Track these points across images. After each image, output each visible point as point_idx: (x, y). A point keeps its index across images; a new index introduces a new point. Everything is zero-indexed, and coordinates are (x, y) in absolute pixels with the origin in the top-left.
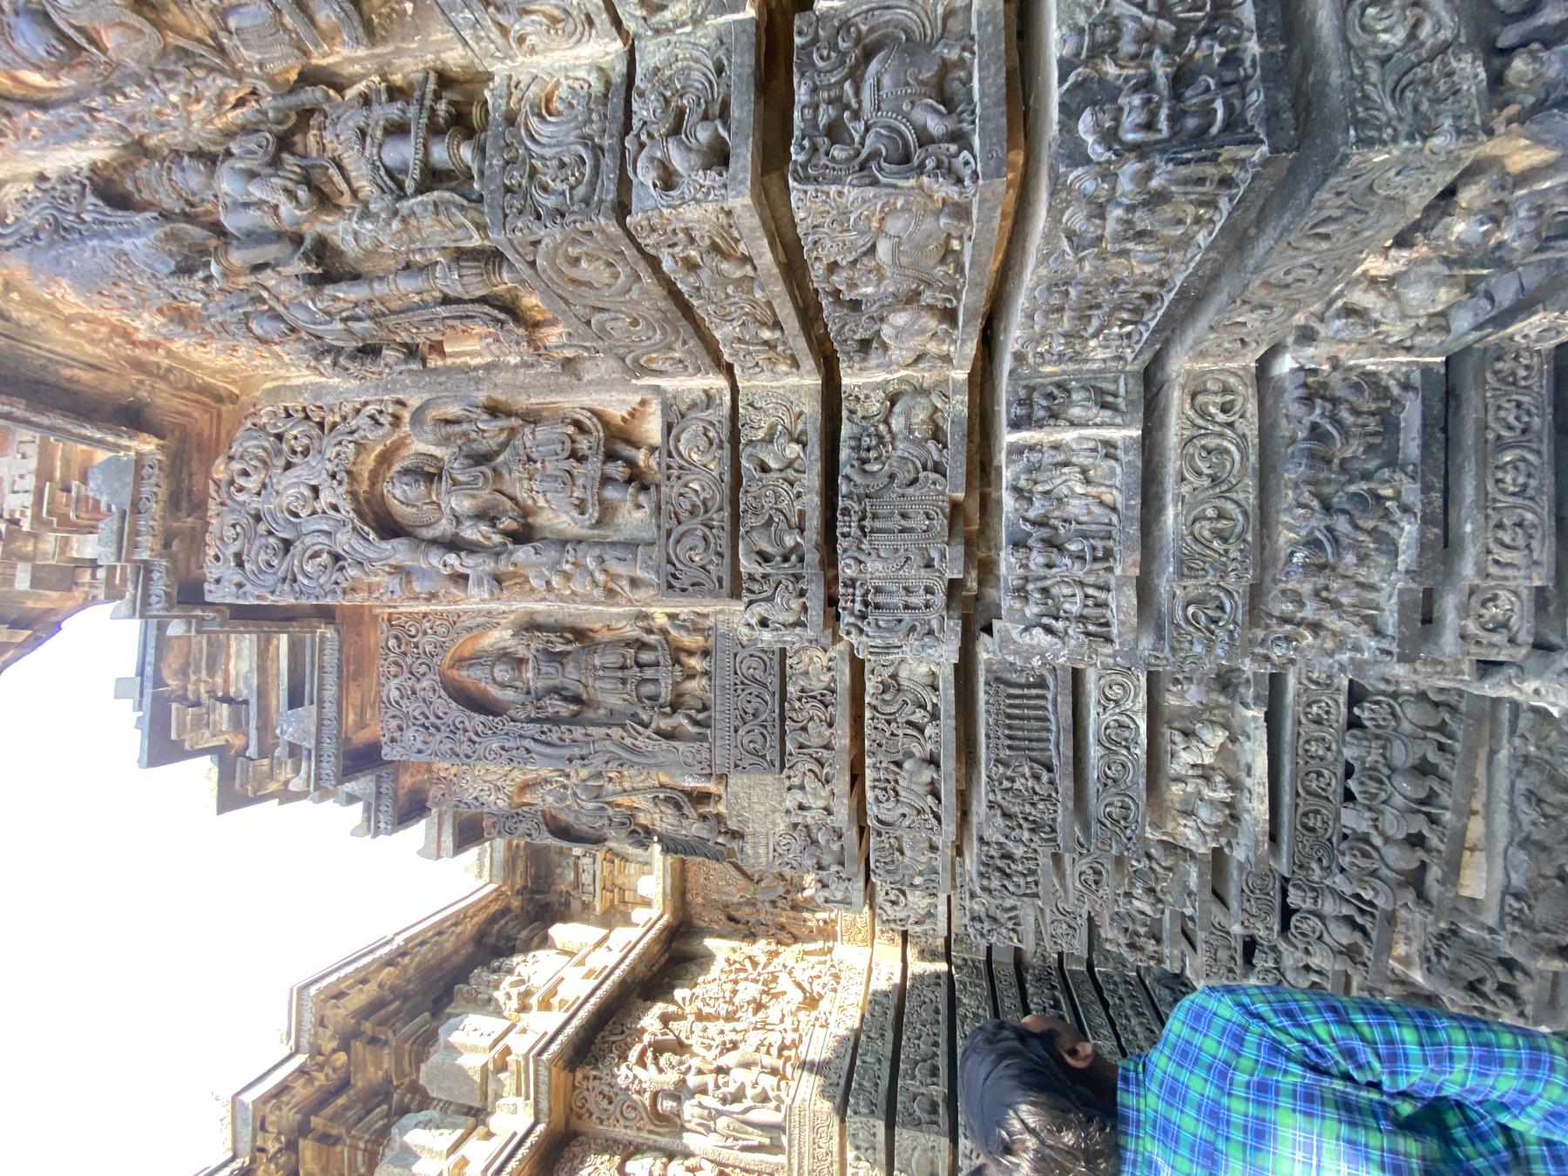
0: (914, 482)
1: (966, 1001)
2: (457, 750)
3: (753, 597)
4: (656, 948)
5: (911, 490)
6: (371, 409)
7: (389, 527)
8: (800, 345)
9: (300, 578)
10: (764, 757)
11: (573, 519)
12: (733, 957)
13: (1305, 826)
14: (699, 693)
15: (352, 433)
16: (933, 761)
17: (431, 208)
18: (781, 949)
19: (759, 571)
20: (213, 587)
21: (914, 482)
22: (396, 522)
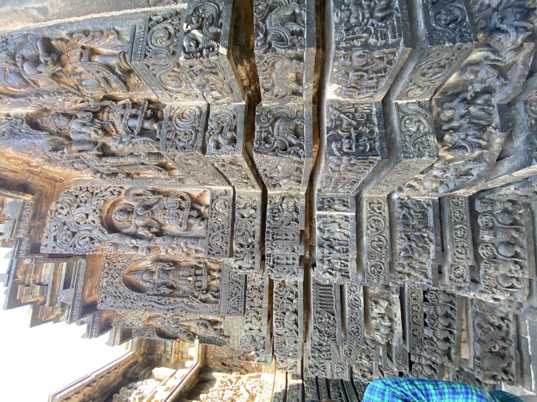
0: (289, 224)
1: (308, 395)
2: (126, 306)
3: (237, 258)
4: (194, 377)
5: (288, 227)
6: (111, 189)
7: (112, 229)
8: (255, 184)
9: (77, 246)
10: (238, 310)
11: (178, 228)
12: (224, 380)
13: (413, 335)
14: (216, 285)
16: (296, 312)
17: (142, 142)
18: (242, 376)
19: (239, 250)
20: (44, 248)
21: (289, 224)
22: (115, 226)
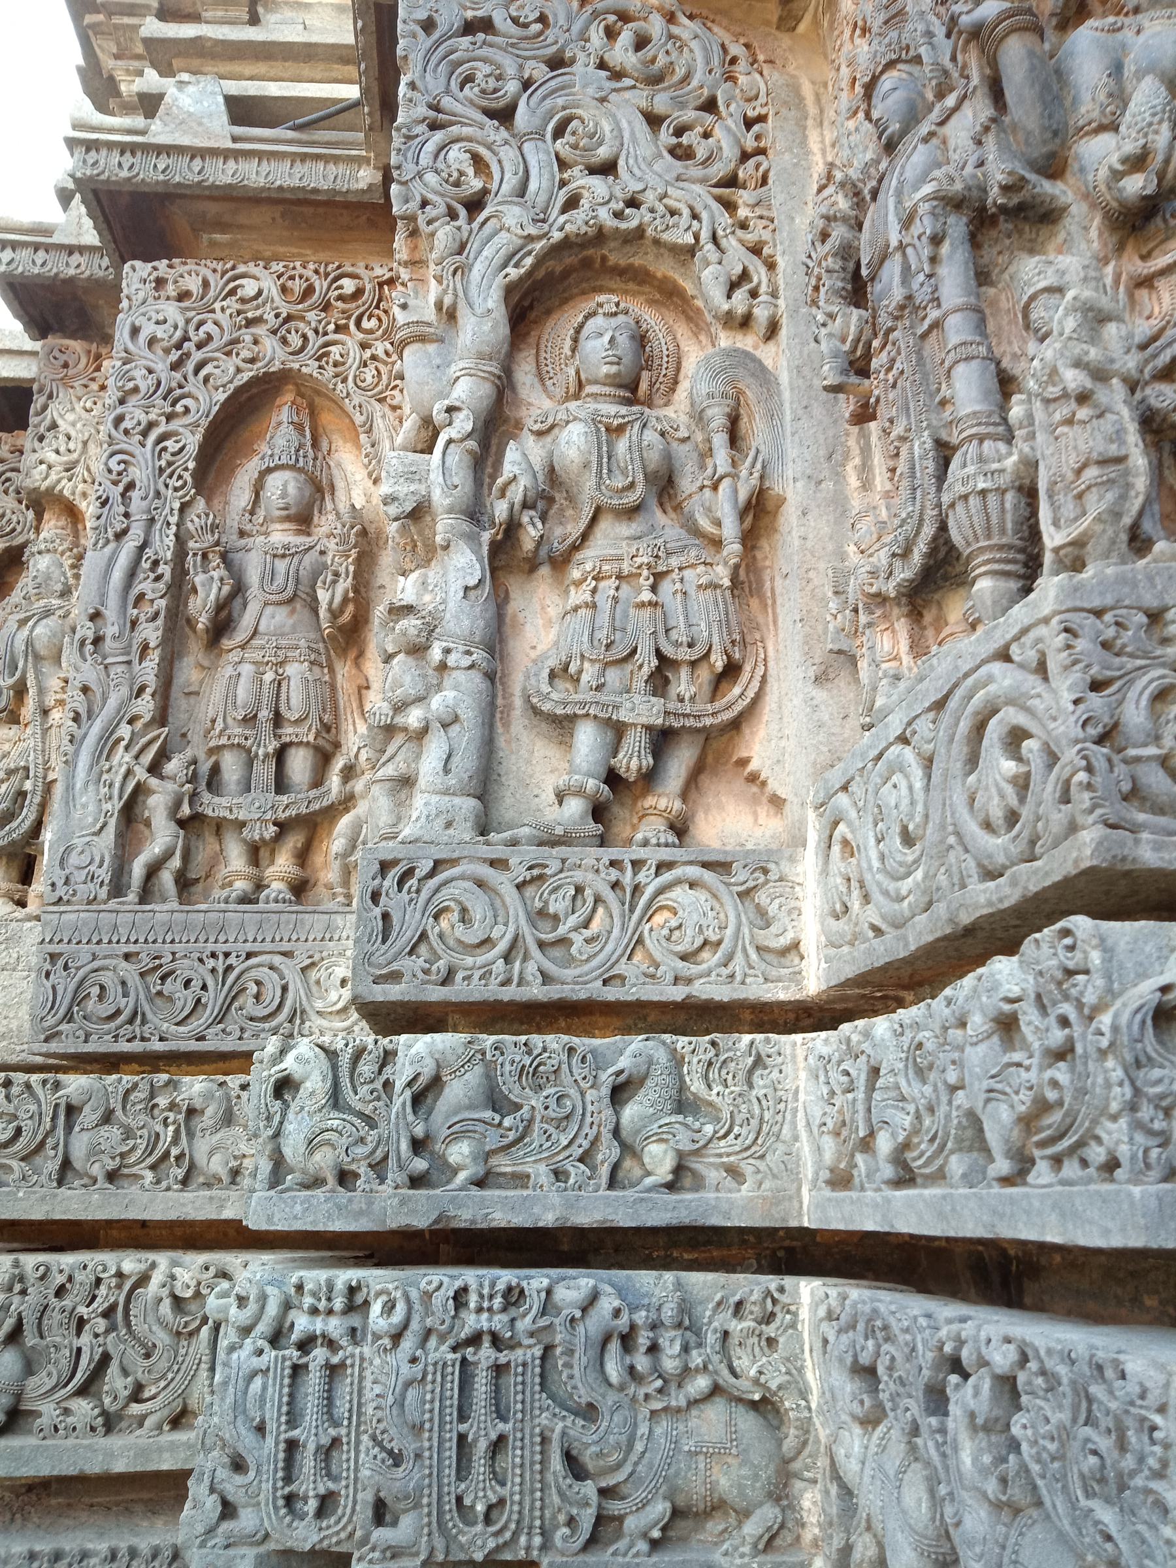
0: (575, 1467)
2: (133, 400)
3: (345, 1060)
5: (556, 1463)
6: (759, 274)
9: (439, 136)
10: (69, 1017)
11: (544, 657)
14: (222, 872)
15: (714, 239)
17: (1113, 450)
19: (401, 1073)
21: (575, 1467)
